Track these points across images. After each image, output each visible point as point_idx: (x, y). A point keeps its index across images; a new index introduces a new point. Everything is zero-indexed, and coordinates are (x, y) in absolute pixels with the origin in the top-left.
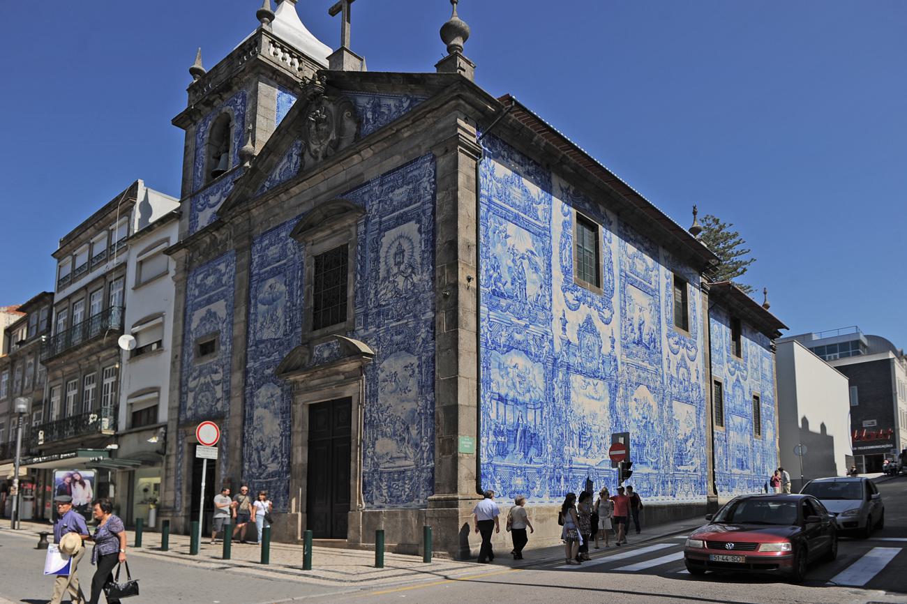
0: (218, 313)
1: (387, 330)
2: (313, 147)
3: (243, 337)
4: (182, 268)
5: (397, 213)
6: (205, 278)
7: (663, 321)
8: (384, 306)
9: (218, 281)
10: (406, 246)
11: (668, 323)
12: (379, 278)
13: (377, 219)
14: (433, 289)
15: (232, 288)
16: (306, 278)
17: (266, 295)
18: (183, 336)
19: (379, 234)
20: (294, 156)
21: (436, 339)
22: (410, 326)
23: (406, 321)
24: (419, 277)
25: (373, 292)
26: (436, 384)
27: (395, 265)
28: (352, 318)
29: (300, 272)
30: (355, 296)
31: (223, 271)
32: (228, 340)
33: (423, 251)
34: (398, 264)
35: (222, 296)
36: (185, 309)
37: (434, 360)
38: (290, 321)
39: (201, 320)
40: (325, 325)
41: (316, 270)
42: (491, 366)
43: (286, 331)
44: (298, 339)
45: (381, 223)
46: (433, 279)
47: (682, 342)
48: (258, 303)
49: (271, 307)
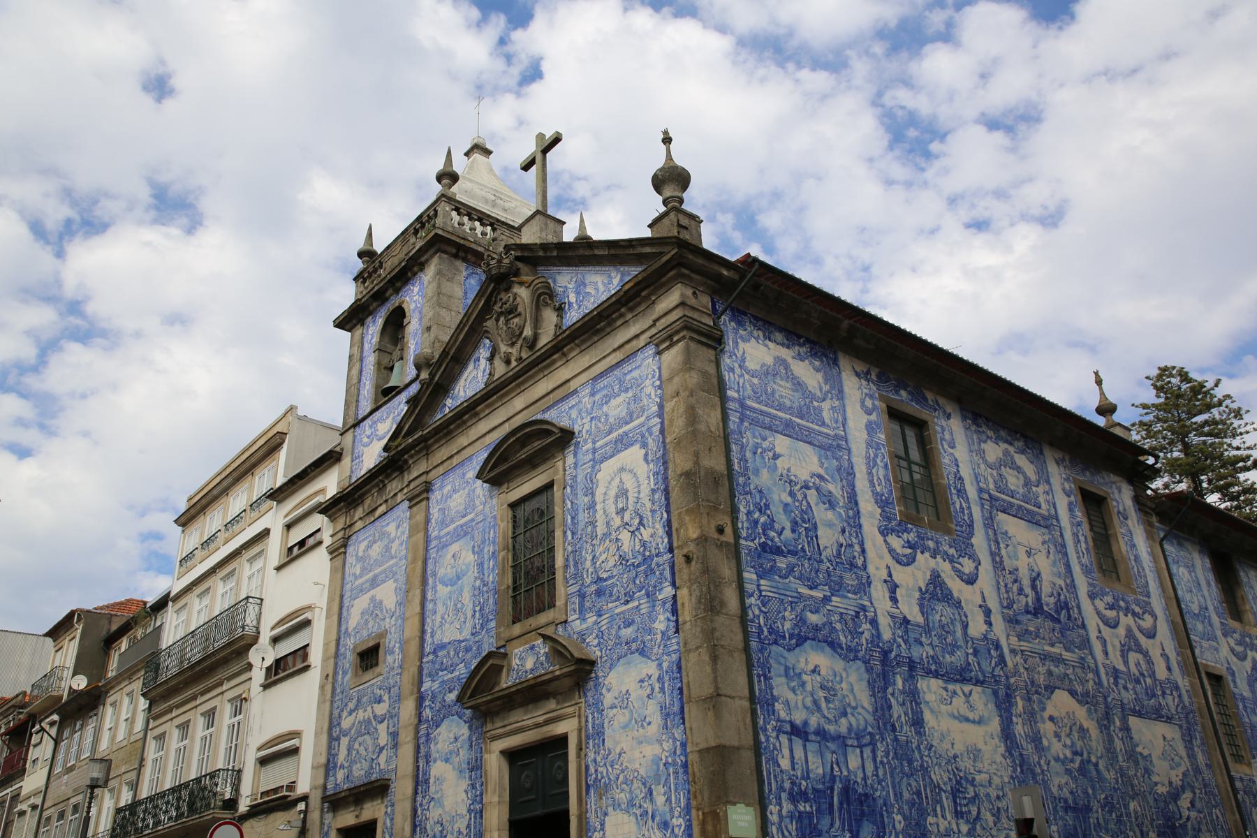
0: (385, 603)
2: (503, 348)
3: (417, 639)
4: (340, 535)
5: (614, 435)
6: (369, 547)
7: (1076, 569)
8: (606, 580)
9: (386, 552)
10: (629, 484)
11: (1087, 571)
12: (596, 536)
14: (671, 550)
15: (404, 561)
17: (449, 570)
18: (338, 640)
19: (593, 467)
20: (481, 360)
21: (680, 632)
22: (643, 611)
23: (636, 603)
24: (650, 531)
25: (589, 558)
26: (686, 710)
27: (617, 513)
28: (563, 601)
29: (492, 532)
30: (566, 566)
31: (393, 535)
32: (397, 645)
33: (653, 491)
34: (621, 512)
37: (679, 668)
39: (362, 613)
40: (529, 615)
41: (514, 527)
42: (772, 674)
43: (475, 627)
45: (594, 451)
46: (669, 534)
47: (1122, 604)
49: (455, 587)
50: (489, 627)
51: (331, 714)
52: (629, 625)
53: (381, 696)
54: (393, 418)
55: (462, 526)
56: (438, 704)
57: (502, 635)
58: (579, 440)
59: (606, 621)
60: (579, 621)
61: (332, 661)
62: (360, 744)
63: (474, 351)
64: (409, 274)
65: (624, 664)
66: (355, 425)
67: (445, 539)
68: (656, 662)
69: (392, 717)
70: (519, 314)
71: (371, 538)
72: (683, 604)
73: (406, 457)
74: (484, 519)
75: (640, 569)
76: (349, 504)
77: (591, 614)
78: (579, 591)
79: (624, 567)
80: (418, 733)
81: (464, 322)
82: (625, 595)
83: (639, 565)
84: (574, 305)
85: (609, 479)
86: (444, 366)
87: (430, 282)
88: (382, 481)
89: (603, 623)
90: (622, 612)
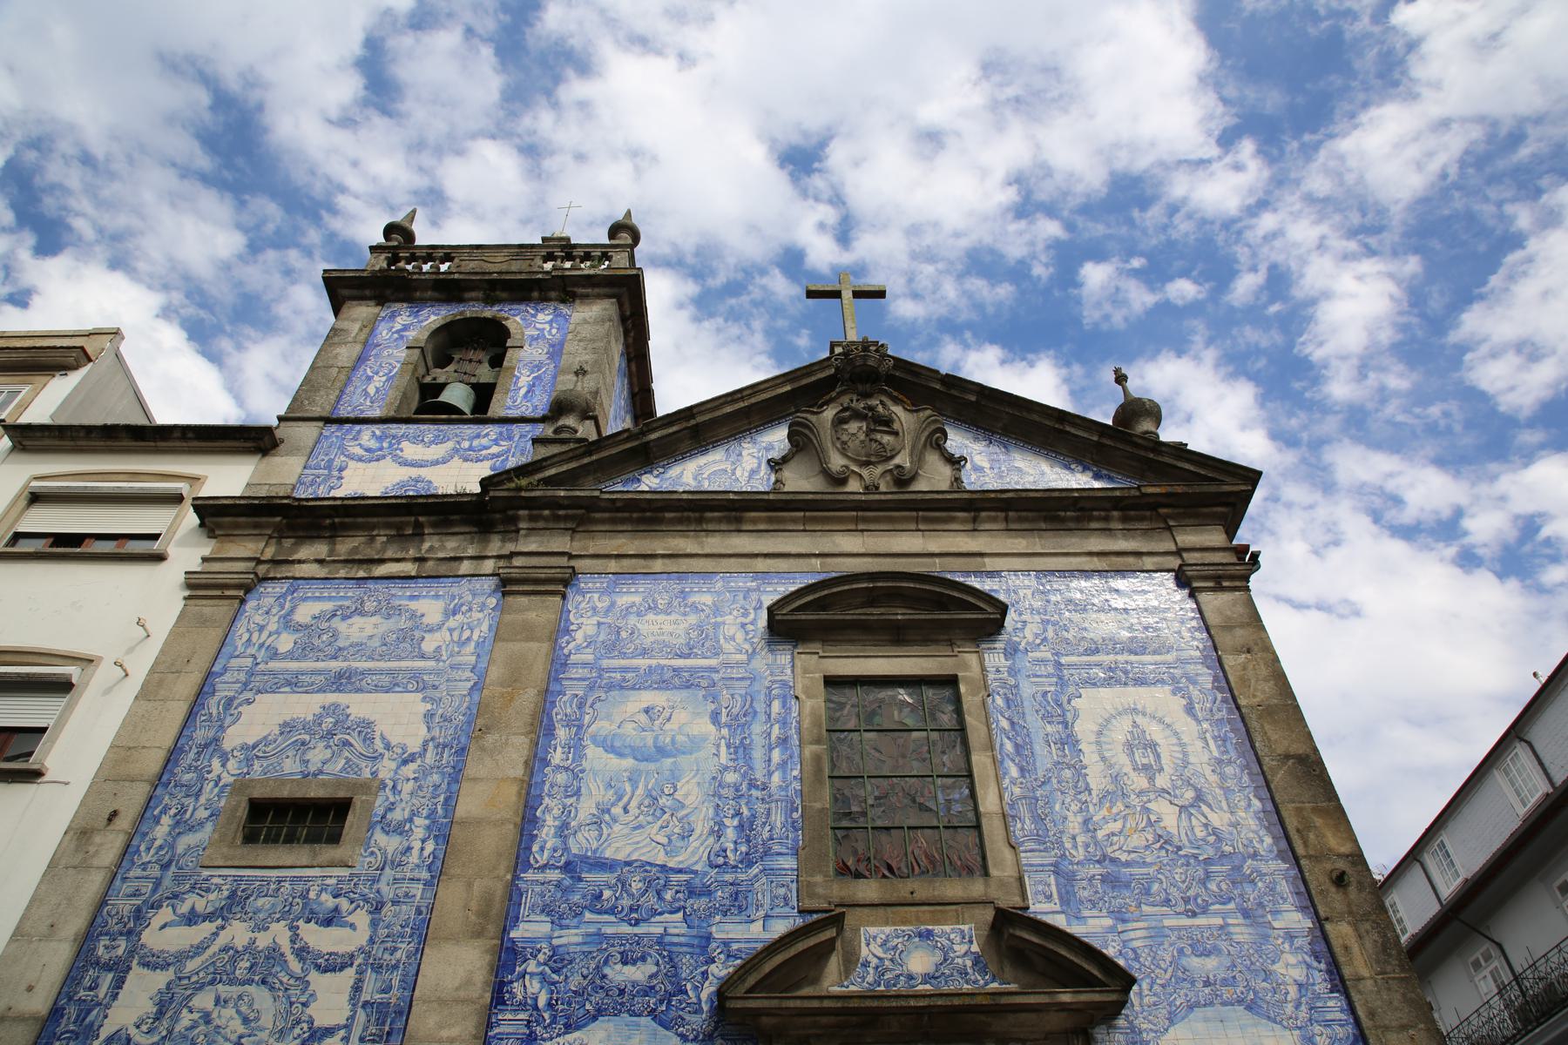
0: (378, 730)
1: (1157, 935)
3: (510, 830)
5: (1106, 659)
10: (1155, 731)
12: (1088, 789)
13: (1049, 655)
15: (468, 674)
16: (806, 723)
18: (173, 755)
23: (1218, 921)
33: (1220, 762)
35: (418, 682)
36: (209, 674)
38: (741, 827)
39: (285, 724)
44: (782, 891)
48: (587, 742)
49: (652, 766)
50: (768, 863)
51: (103, 903)
52: (1207, 954)
53: (336, 909)
54: (455, 451)
55: (677, 671)
56: (575, 982)
57: (820, 890)
58: (1015, 639)
59: (1139, 933)
60: (1063, 916)
61: (140, 792)
62: (220, 1002)
63: (727, 438)
64: (535, 294)
65: (1206, 1020)
66: (328, 421)
67: (618, 676)
68: (1297, 1032)
69: (378, 968)
70: (896, 434)
71: (347, 603)
72: (1346, 948)
73: (522, 512)
74: (753, 679)
75: (1214, 868)
76: (291, 527)
77: (1095, 912)
78: (1056, 865)
79: (1175, 856)
80: (489, 1026)
81: (745, 393)
82: (1186, 901)
83: (1208, 861)
84: (988, 471)
85: (1107, 716)
86: (675, 429)
87: (585, 322)
88: (418, 526)
89: (1132, 935)
90: (1185, 928)
